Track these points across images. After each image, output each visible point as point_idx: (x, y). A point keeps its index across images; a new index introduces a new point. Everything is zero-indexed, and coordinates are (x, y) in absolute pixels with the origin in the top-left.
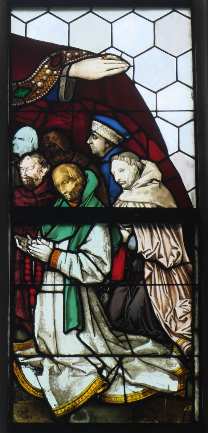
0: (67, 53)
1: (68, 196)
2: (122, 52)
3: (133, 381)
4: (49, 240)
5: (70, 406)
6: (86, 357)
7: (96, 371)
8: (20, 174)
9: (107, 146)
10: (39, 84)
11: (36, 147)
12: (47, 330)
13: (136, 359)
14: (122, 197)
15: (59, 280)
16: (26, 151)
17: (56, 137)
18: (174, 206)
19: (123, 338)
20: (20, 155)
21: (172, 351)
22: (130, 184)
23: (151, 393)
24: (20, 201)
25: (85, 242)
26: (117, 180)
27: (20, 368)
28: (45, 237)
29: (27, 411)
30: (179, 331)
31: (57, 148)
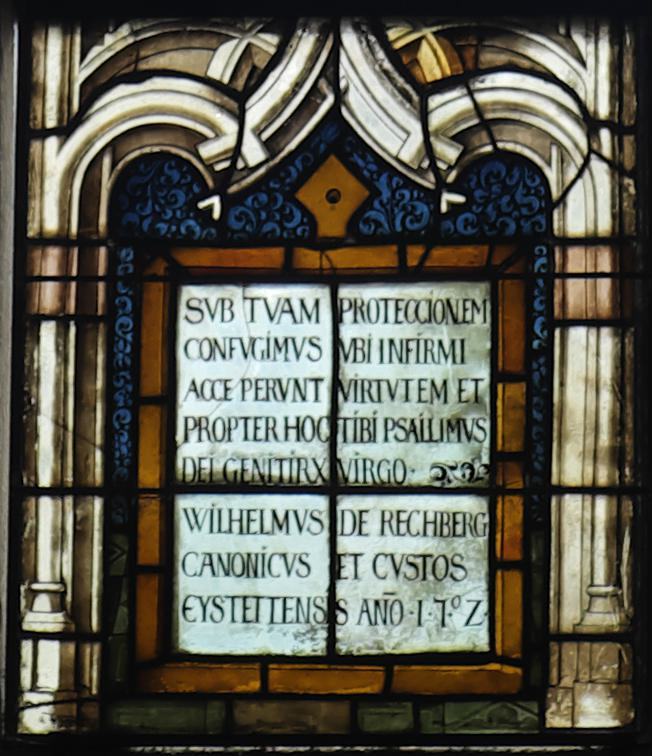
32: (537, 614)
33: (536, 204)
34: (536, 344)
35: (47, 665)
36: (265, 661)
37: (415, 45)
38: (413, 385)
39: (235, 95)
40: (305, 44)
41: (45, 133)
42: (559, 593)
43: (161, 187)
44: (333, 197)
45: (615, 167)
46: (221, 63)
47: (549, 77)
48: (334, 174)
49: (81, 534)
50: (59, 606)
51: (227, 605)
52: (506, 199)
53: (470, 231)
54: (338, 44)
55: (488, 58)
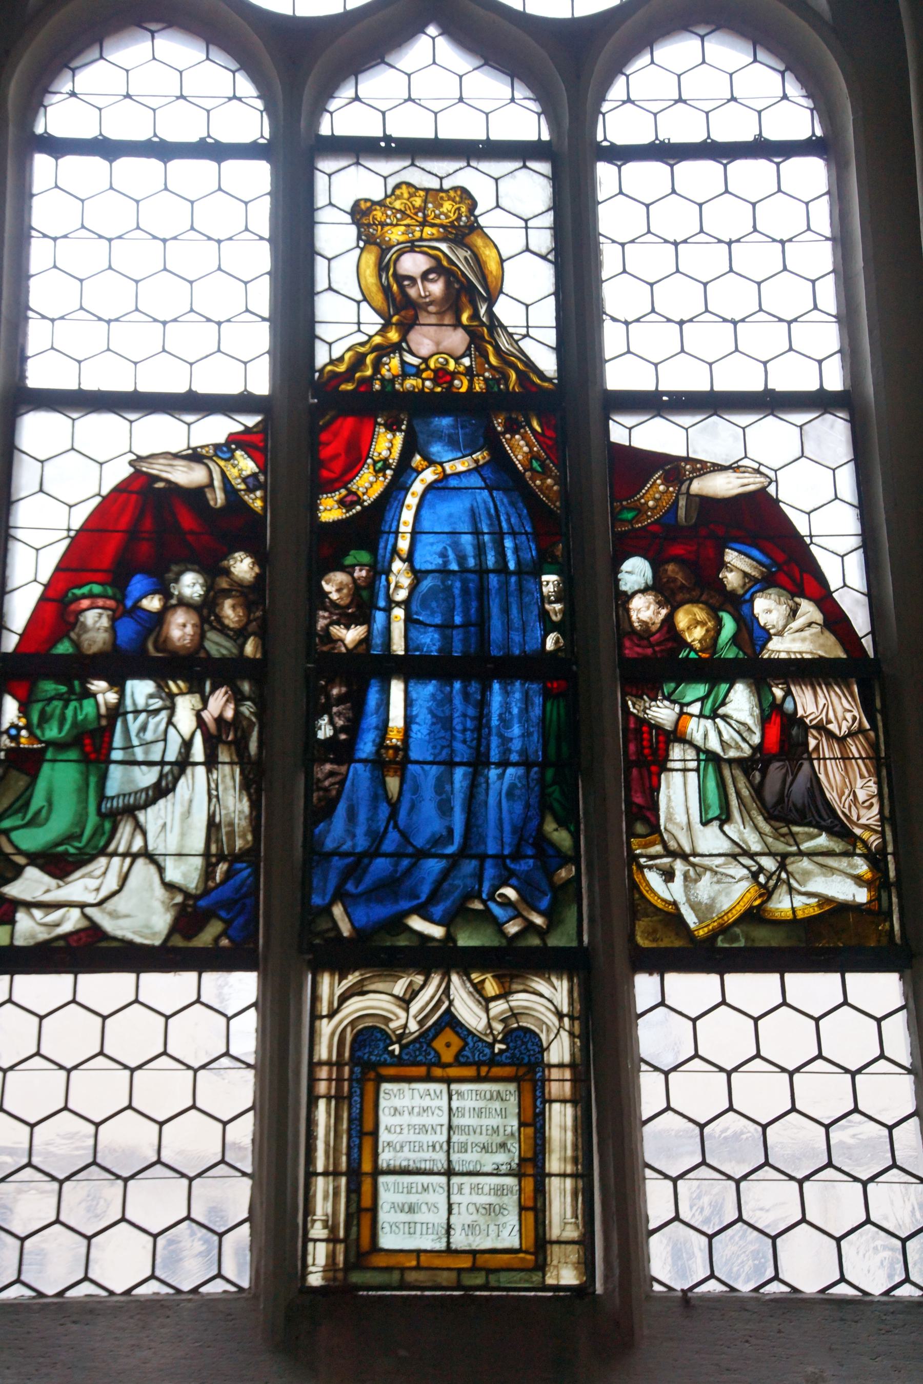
0: (686, 464)
1: (697, 645)
2: (760, 464)
3: (803, 889)
4: (674, 702)
5: (715, 924)
6: (734, 856)
7: (750, 875)
8: (629, 617)
9: (747, 581)
10: (651, 503)
11: (650, 582)
12: (678, 821)
13: (805, 859)
14: (771, 645)
15: (691, 754)
16: (636, 588)
17: (677, 569)
18: (843, 656)
19: (784, 830)
20: (629, 593)
21: (855, 847)
22: (780, 628)
23: (828, 905)
24: (631, 651)
25: (723, 704)
26: (762, 624)
27: (642, 873)
28: (668, 698)
29: (655, 931)
30: (863, 821)
31: (679, 584)
32: (541, 1231)
33: (537, 1050)
34: (538, 1110)
35: (319, 1254)
36: (418, 1252)
37: (483, 981)
38: (484, 1128)
39: (405, 1002)
40: (435, 980)
41: (323, 1017)
42: (550, 1222)
43: (373, 1040)
44: (448, 1045)
45: (571, 1034)
46: (400, 987)
47: (542, 995)
48: (448, 1035)
49: (336, 1194)
50: (326, 1226)
51: (401, 1226)
52: (523, 1047)
53: (508, 1061)
54: (449, 981)
55: (515, 987)
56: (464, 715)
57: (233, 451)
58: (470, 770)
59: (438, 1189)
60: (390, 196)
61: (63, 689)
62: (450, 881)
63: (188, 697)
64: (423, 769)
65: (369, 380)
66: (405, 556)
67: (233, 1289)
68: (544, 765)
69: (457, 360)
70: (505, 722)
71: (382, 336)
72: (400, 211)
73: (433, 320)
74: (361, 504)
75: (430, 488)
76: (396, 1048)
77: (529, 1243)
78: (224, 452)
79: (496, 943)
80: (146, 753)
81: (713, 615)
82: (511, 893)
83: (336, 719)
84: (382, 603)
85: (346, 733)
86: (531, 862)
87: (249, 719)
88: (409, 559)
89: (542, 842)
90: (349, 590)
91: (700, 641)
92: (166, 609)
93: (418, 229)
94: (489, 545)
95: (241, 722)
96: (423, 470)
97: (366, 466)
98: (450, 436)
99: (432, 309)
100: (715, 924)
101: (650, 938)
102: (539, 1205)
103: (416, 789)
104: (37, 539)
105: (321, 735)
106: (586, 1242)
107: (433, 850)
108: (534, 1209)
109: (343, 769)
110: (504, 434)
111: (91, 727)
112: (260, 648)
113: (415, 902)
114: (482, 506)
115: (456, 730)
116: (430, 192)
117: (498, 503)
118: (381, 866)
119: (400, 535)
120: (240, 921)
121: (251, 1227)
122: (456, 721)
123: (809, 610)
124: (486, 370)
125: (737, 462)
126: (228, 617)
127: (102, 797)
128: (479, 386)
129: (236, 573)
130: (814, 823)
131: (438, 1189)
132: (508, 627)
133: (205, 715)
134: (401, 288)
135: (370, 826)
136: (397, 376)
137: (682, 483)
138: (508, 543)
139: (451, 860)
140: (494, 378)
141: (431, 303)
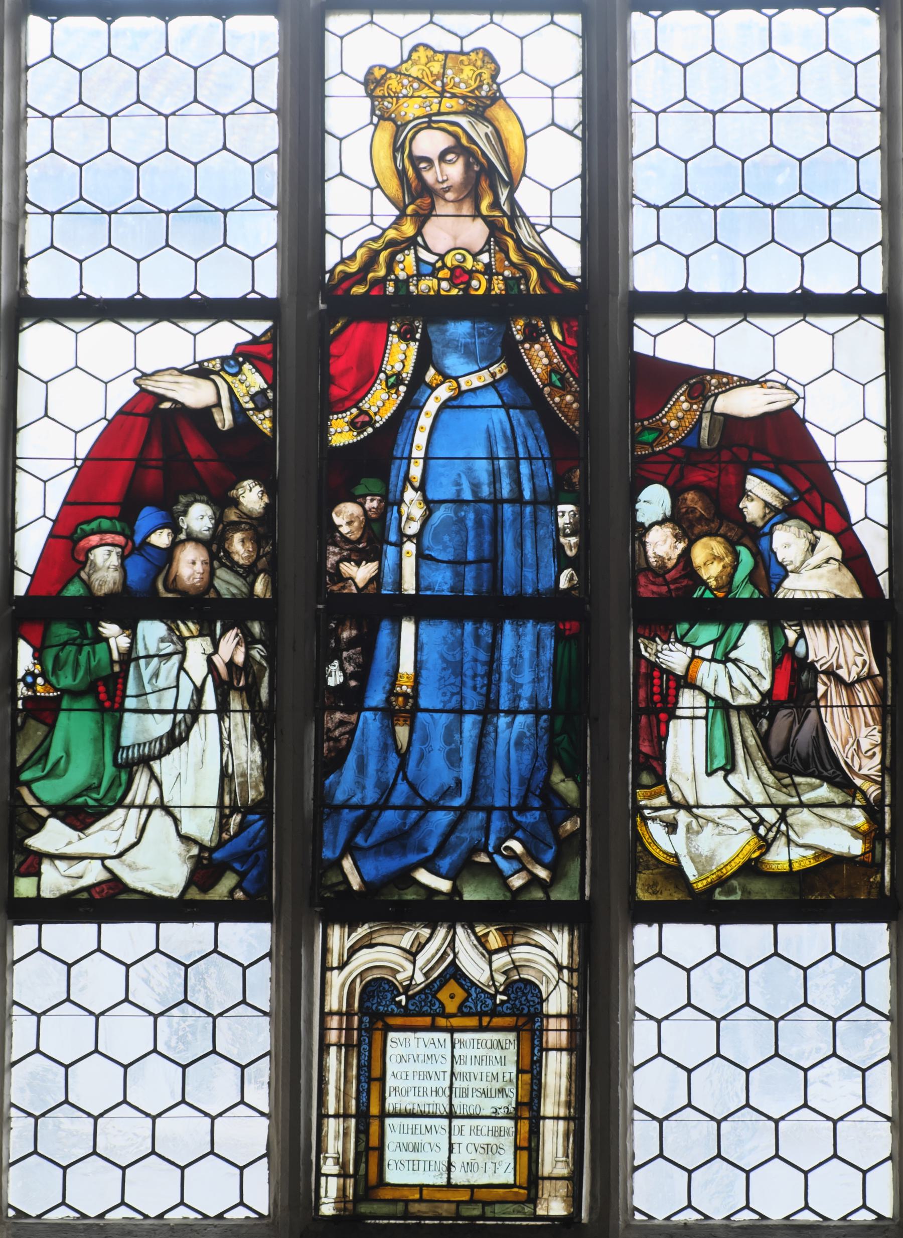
0: (712, 378)
1: (713, 583)
2: (789, 378)
3: (801, 841)
4: (686, 645)
5: (714, 876)
6: (736, 808)
7: (750, 827)
8: (646, 552)
9: (767, 511)
10: (673, 424)
11: (668, 513)
12: (683, 771)
13: (805, 810)
14: (787, 584)
15: (701, 700)
16: (654, 520)
17: (696, 498)
18: (859, 595)
19: (787, 781)
20: (647, 525)
21: (854, 798)
22: (798, 564)
23: (825, 857)
24: (647, 589)
25: (735, 647)
26: (780, 560)
27: (646, 825)
28: (680, 641)
29: (655, 884)
30: (864, 771)
31: (698, 515)
32: (534, 1168)
33: (536, 1000)
34: (535, 1058)
35: (330, 1189)
36: (421, 1187)
37: (487, 934)
38: (484, 1075)
39: (412, 954)
40: (441, 932)
41: (332, 969)
42: (543, 1160)
43: (380, 992)
44: (452, 997)
45: (570, 986)
46: (407, 940)
47: (543, 948)
48: (452, 987)
49: (346, 1134)
50: (337, 1161)
51: (406, 1164)
52: (524, 998)
53: (509, 1011)
54: (455, 933)
55: (518, 940)
56: (475, 660)
57: (240, 365)
58: (480, 718)
59: (440, 1130)
60: (406, 61)
61: (76, 633)
62: (457, 834)
63: (199, 640)
64: (432, 717)
65: (383, 281)
66: (417, 484)
67: (254, 1216)
68: (553, 713)
69: (475, 256)
70: (515, 666)
71: (396, 229)
72: (417, 79)
73: (450, 209)
74: (373, 426)
75: (445, 406)
76: (403, 998)
77: (523, 1179)
78: (232, 367)
79: (500, 898)
80: (159, 701)
81: (730, 549)
82: (516, 846)
83: (347, 665)
84: (393, 537)
85: (356, 680)
86: (537, 814)
87: (260, 664)
88: (422, 488)
89: (548, 793)
90: (361, 523)
91: (716, 579)
92: (175, 544)
93: (436, 100)
94: (504, 471)
95: (252, 667)
96: (438, 386)
97: (378, 381)
98: (466, 346)
99: (450, 196)
100: (714, 876)
101: (650, 891)
102: (533, 1145)
103: (426, 739)
104: (45, 470)
105: (331, 682)
106: (575, 1178)
107: (441, 802)
108: (529, 1149)
109: (353, 718)
110: (522, 342)
111: (104, 674)
112: (270, 587)
113: (423, 856)
114: (498, 427)
115: (465, 675)
116: (450, 56)
117: (515, 423)
118: (389, 819)
119: (412, 461)
120: (254, 872)
121: (269, 1163)
122: (466, 666)
123: (828, 545)
124: (505, 268)
125: (764, 376)
126: (237, 553)
127: (117, 747)
128: (498, 286)
129: (245, 504)
130: (817, 773)
131: (440, 1130)
132: (522, 565)
133: (215, 658)
134: (417, 171)
135: (379, 779)
136: (413, 276)
137: (706, 399)
138: (524, 468)
139: (458, 813)
140: (513, 278)
141: (448, 189)
